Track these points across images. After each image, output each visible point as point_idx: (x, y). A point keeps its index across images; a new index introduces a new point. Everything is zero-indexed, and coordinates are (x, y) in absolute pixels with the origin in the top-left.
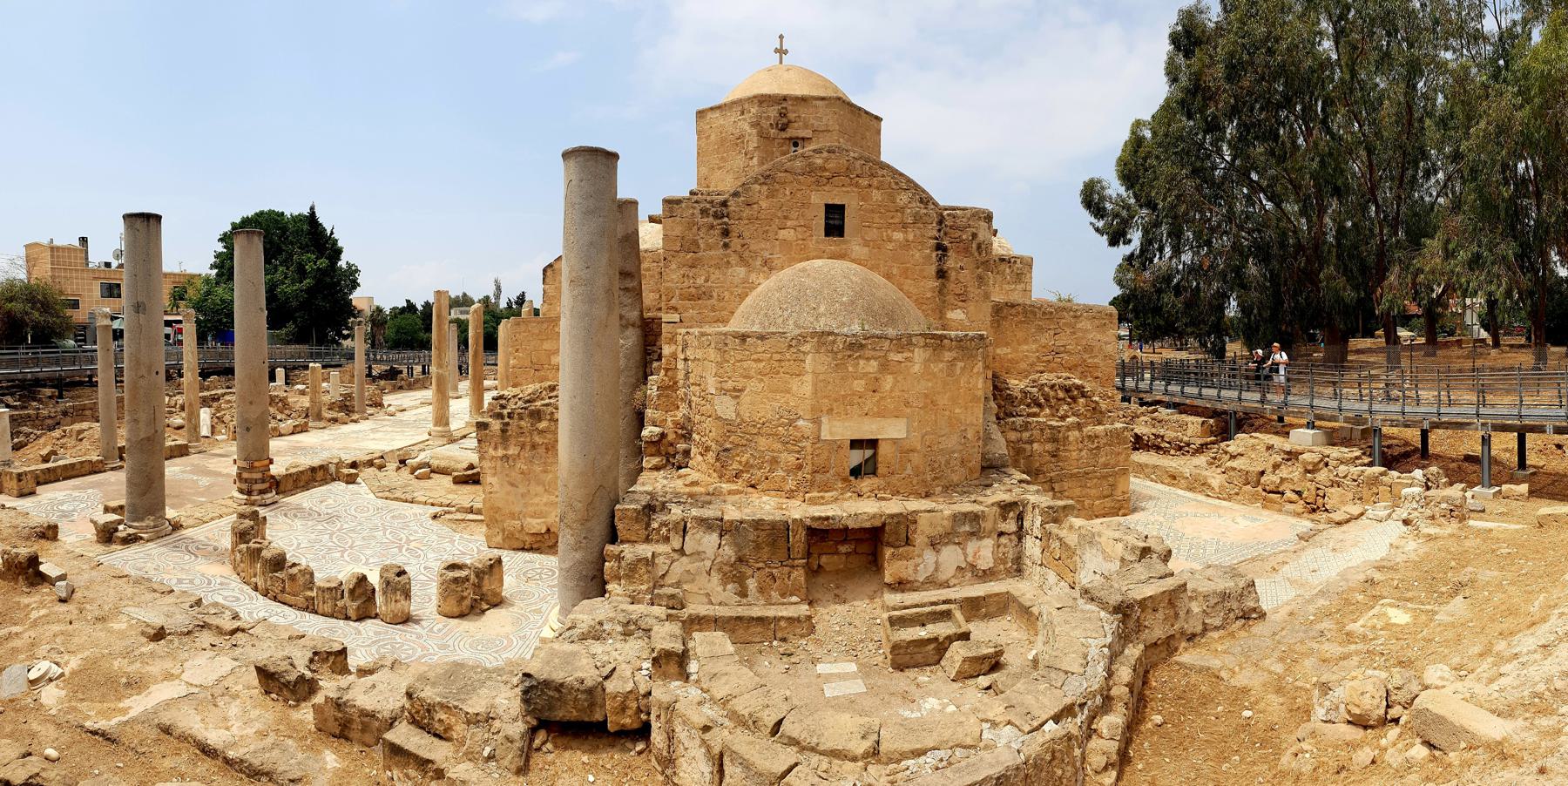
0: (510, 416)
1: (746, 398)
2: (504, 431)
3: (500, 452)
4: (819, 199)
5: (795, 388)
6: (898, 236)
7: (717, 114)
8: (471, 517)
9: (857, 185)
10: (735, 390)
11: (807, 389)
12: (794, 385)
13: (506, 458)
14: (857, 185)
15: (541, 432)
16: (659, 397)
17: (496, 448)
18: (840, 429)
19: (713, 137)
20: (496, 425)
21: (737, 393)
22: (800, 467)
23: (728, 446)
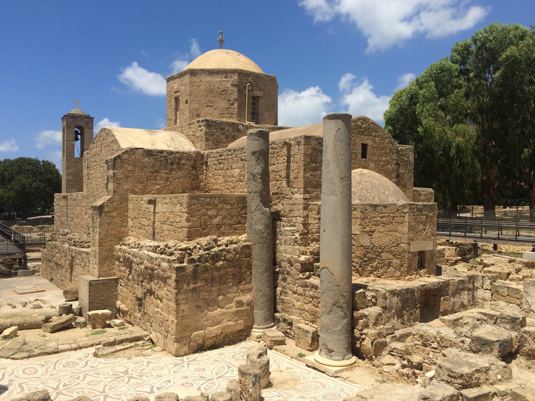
0: (199, 260)
1: (375, 235)
2: (195, 271)
3: (192, 286)
4: (359, 141)
5: (400, 229)
6: (384, 159)
8: (118, 347)
9: (372, 136)
10: (370, 231)
11: (406, 229)
12: (400, 228)
13: (194, 290)
14: (372, 136)
15: (219, 269)
16: (301, 239)
17: (188, 284)
18: (415, 247)
19: (202, 87)
20: (190, 268)
21: (371, 233)
22: (402, 266)
23: (365, 259)
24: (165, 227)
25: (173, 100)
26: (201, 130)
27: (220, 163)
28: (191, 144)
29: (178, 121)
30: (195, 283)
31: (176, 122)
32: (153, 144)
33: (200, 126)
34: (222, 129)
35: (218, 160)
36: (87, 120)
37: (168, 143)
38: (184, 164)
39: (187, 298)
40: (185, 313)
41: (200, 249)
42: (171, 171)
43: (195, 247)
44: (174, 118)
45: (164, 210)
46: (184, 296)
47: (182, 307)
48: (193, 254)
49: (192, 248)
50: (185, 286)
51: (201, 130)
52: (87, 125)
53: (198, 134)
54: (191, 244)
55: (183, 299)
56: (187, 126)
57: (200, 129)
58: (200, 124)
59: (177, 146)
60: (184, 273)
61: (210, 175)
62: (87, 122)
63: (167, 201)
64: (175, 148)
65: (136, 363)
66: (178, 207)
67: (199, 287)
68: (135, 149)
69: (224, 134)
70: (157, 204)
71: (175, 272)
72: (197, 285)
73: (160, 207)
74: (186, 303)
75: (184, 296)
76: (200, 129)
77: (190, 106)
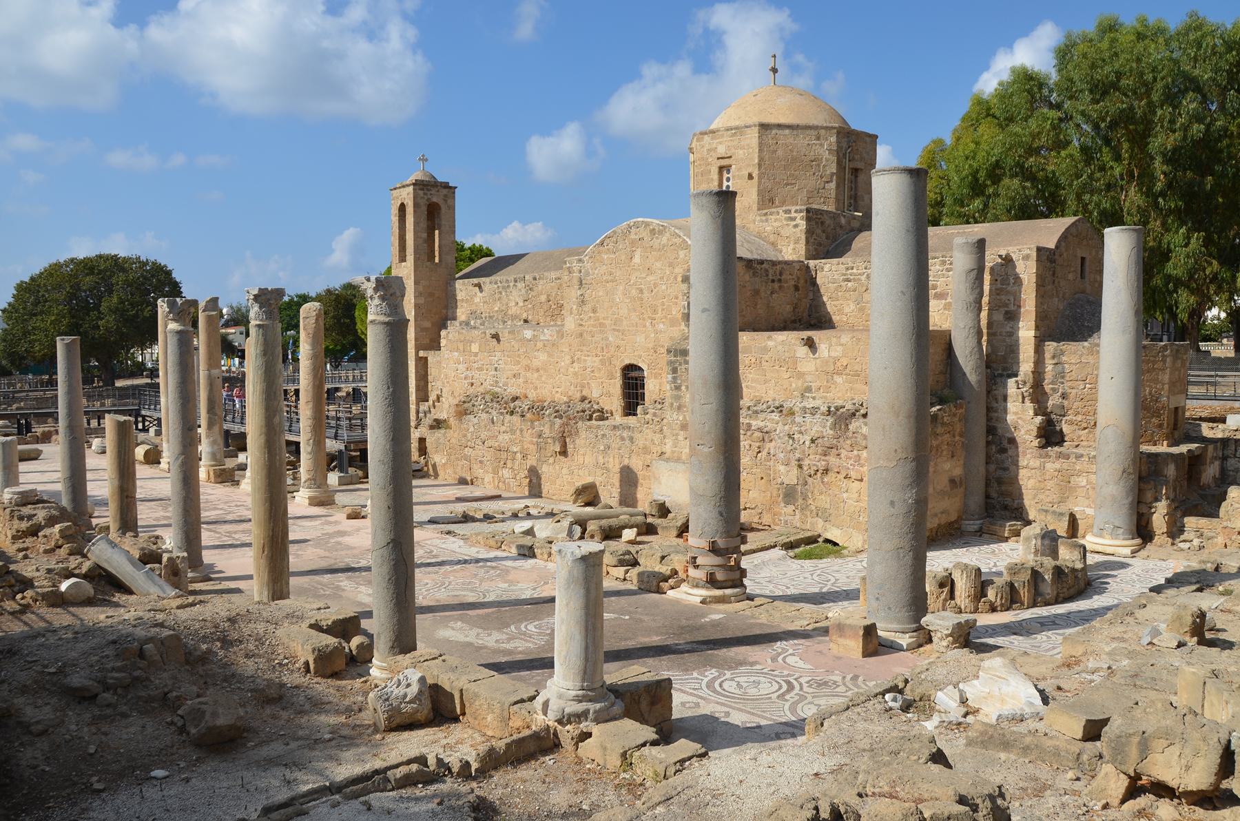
7: (787, 132)
19: (780, 153)
24: (839, 379)
25: (715, 170)
27: (849, 281)
33: (794, 219)
36: (445, 191)
45: (833, 354)
52: (445, 201)
53: (788, 231)
58: (793, 215)
62: (446, 196)
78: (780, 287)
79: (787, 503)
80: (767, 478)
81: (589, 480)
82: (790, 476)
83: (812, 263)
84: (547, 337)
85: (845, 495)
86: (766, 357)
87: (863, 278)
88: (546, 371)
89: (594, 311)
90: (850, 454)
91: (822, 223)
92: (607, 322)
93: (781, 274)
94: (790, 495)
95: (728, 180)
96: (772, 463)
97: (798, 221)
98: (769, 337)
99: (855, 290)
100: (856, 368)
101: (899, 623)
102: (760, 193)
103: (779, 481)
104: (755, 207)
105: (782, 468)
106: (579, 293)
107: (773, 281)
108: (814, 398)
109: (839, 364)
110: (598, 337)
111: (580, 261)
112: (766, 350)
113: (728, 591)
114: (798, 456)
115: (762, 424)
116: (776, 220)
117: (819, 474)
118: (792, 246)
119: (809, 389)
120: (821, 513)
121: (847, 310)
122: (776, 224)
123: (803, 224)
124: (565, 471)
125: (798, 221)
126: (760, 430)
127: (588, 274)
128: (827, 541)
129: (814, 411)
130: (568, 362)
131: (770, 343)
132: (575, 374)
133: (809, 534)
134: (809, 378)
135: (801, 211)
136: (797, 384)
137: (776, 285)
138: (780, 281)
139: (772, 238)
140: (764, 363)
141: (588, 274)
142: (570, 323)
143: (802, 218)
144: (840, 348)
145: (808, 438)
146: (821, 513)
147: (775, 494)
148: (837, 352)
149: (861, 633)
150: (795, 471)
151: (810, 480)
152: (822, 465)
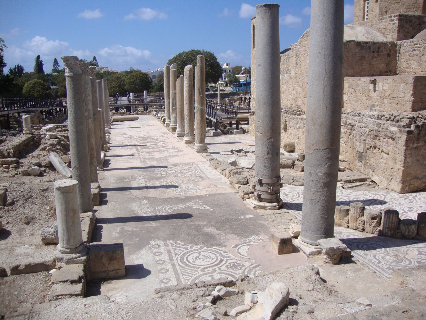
2: (419, 134)
3: (415, 145)
13: (417, 147)
17: (413, 144)
24: (386, 101)
26: (394, 24)
27: (415, 50)
28: (382, 35)
29: (366, 17)
30: (418, 143)
31: (364, 18)
32: (357, 37)
33: (392, 20)
34: (410, 22)
35: (413, 48)
37: (366, 35)
38: (382, 52)
39: (411, 154)
40: (409, 164)
41: (421, 118)
42: (373, 58)
43: (418, 117)
44: (362, 15)
45: (384, 88)
46: (409, 152)
47: (408, 160)
48: (417, 122)
49: (416, 117)
50: (411, 145)
51: (394, 24)
53: (390, 27)
54: (415, 115)
55: (409, 154)
56: (378, 21)
57: (393, 22)
58: (393, 18)
59: (373, 38)
60: (411, 135)
61: (403, 60)
63: (389, 81)
64: (372, 39)
65: (376, 195)
66: (402, 86)
67: (420, 146)
68: (349, 41)
69: (411, 26)
70: (377, 84)
71: (406, 134)
72: (419, 145)
73: (379, 86)
74: (410, 157)
75: (409, 152)
76: (393, 22)
77: (380, 4)
78: (378, 55)
79: (360, 161)
80: (353, 148)
81: (292, 141)
82: (361, 148)
83: (399, 42)
84: (286, 79)
85: (381, 160)
86: (358, 89)
87: (422, 49)
88: (285, 93)
89: (300, 67)
90: (384, 140)
91: (410, 22)
92: (304, 72)
93: (379, 48)
94: (361, 156)
95: (368, 4)
96: (354, 141)
97: (395, 21)
98: (359, 80)
99: (417, 56)
100: (393, 96)
101: (310, 239)
102: (380, 9)
103: (357, 149)
104: (377, 16)
105: (358, 143)
106: (296, 59)
107: (374, 52)
108: (375, 110)
109: (386, 93)
110: (301, 79)
111: (296, 45)
112: (357, 86)
113: (267, 204)
114: (364, 138)
115: (351, 121)
116: (385, 22)
117: (372, 148)
118: (391, 34)
119: (373, 106)
120: (371, 167)
121: (413, 66)
122: (385, 24)
123: (397, 22)
124: (286, 136)
125: (395, 21)
126: (350, 124)
127: (298, 51)
128: (373, 181)
129: (372, 117)
130: (292, 89)
131: (360, 82)
132: (294, 94)
133: (364, 177)
134: (374, 100)
135: (396, 16)
136: (369, 103)
137: (376, 54)
138: (378, 52)
139: (383, 31)
140: (357, 92)
141: (298, 51)
142: (293, 73)
143: (396, 20)
144: (387, 85)
145: (367, 130)
146: (371, 167)
147: (355, 156)
148: (386, 87)
149: (279, 241)
150: (363, 145)
151: (368, 151)
152: (373, 144)
